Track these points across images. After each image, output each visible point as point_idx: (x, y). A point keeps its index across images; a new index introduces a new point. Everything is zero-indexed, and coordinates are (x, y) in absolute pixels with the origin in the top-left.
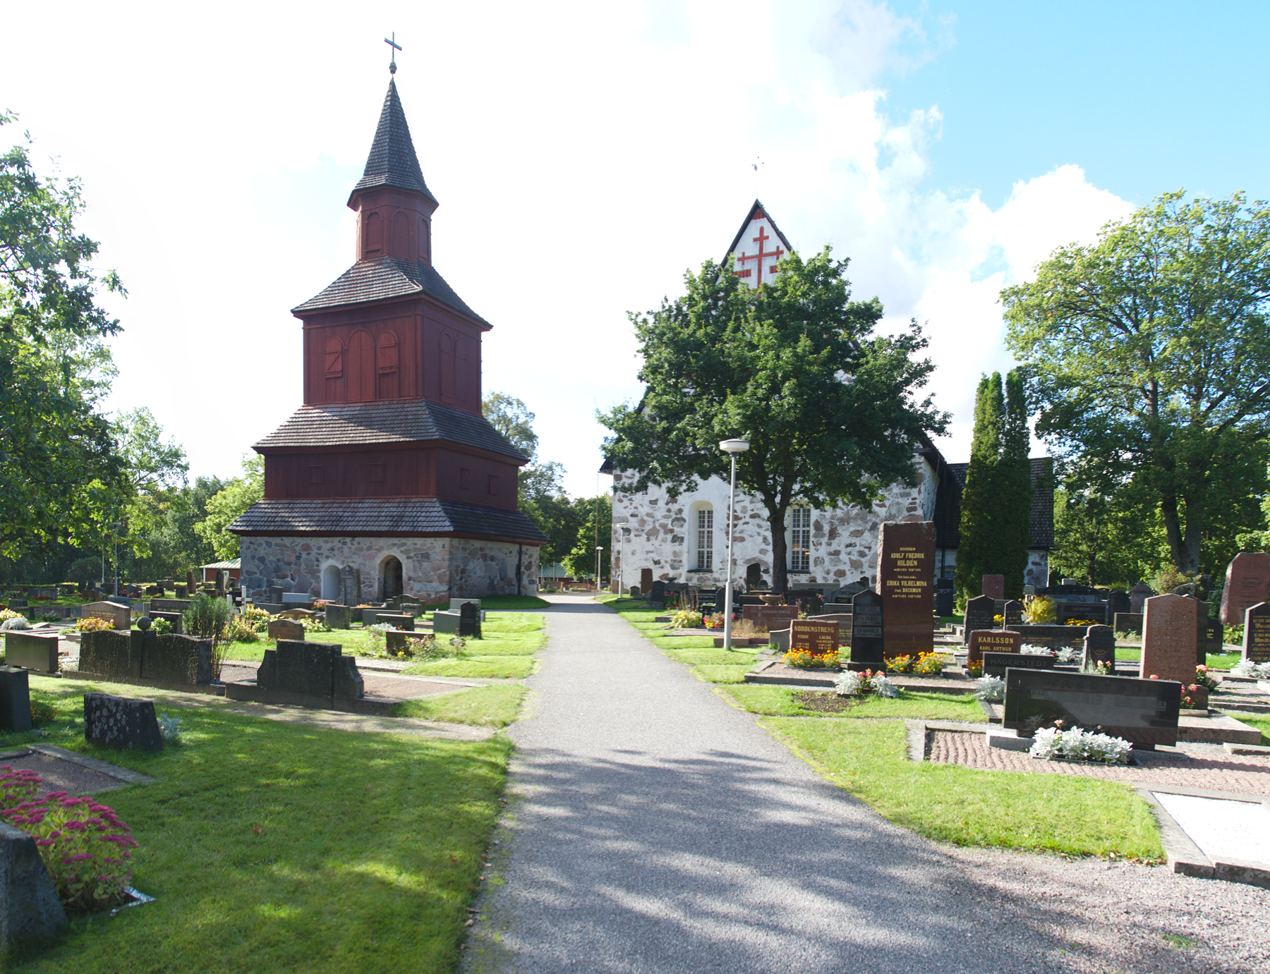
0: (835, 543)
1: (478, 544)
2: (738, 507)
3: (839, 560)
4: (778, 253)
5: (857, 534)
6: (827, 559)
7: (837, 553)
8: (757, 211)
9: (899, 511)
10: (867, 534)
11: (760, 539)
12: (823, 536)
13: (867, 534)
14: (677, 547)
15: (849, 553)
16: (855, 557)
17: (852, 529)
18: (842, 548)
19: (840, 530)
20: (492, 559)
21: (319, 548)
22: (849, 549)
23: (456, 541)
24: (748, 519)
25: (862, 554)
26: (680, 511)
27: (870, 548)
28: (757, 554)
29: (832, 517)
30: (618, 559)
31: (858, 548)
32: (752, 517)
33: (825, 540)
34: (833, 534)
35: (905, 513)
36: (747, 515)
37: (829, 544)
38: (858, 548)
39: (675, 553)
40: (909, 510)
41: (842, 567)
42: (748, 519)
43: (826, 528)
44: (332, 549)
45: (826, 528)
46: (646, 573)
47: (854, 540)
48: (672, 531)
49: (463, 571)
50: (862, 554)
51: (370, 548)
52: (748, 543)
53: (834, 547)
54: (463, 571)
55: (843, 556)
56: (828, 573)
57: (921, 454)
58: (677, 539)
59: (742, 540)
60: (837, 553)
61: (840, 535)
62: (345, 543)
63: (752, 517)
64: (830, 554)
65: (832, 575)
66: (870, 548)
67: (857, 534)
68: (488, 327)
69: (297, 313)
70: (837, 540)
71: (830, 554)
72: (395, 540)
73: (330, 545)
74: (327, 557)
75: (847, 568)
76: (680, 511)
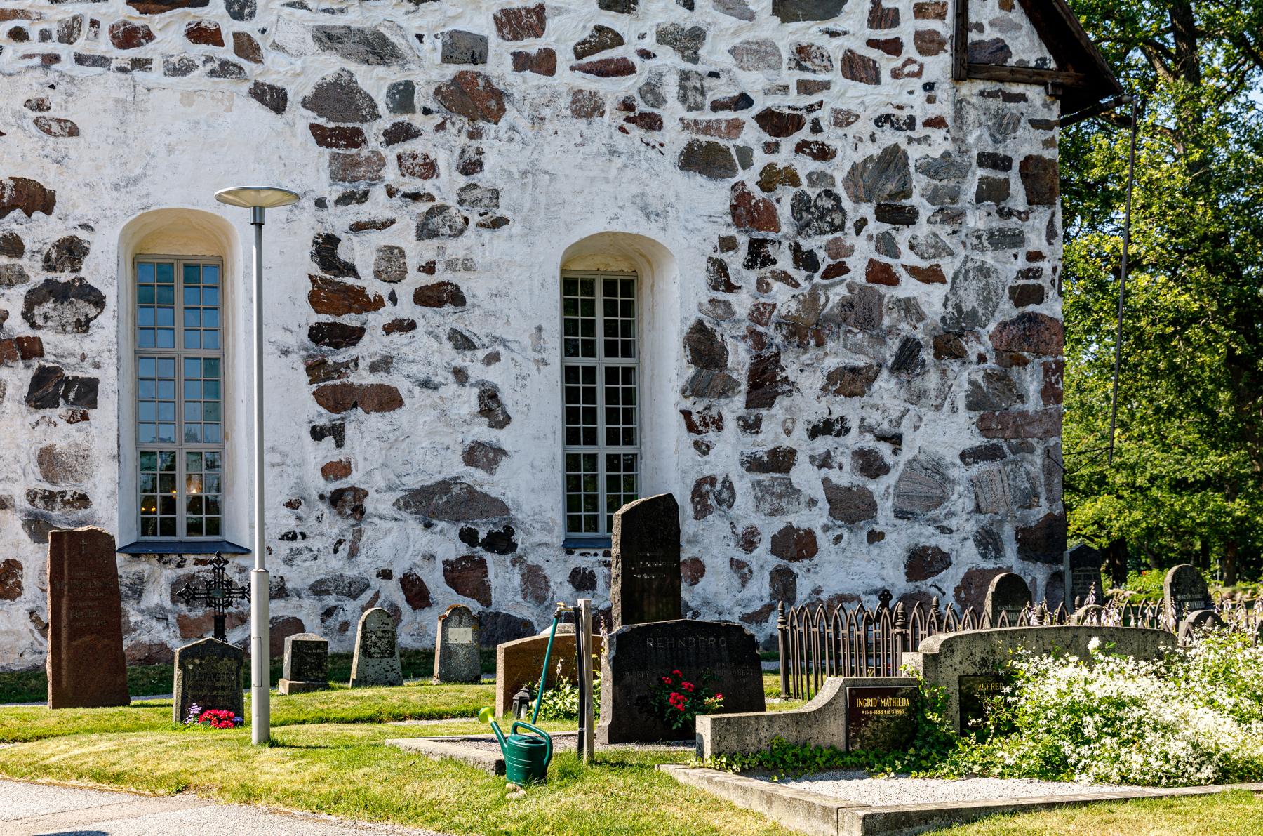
0: (774, 417)
2: (360, 253)
3: (791, 492)
5: (851, 382)
6: (743, 484)
7: (781, 461)
9: (987, 298)
10: (885, 385)
11: (469, 400)
12: (728, 389)
13: (885, 385)
14: (59, 431)
15: (825, 461)
16: (845, 476)
17: (832, 363)
18: (798, 440)
19: (791, 365)
22: (823, 444)
24: (406, 308)
25: (871, 465)
26: (72, 251)
28: (455, 467)
29: (759, 314)
31: (854, 440)
32: (425, 297)
33: (733, 407)
34: (765, 384)
35: (1008, 310)
36: (406, 290)
37: (751, 426)
38: (854, 440)
39: (48, 460)
41: (801, 519)
42: (406, 308)
43: (739, 358)
45: (739, 358)
47: (841, 407)
50: (871, 465)
52: (416, 414)
53: (770, 437)
55: (805, 476)
56: (749, 541)
58: (56, 390)
59: (388, 400)
60: (781, 461)
61: (793, 388)
63: (425, 297)
64: (753, 464)
65: (763, 548)
66: (896, 440)
67: (851, 382)
70: (781, 405)
71: (753, 464)
75: (815, 519)
76: (72, 251)
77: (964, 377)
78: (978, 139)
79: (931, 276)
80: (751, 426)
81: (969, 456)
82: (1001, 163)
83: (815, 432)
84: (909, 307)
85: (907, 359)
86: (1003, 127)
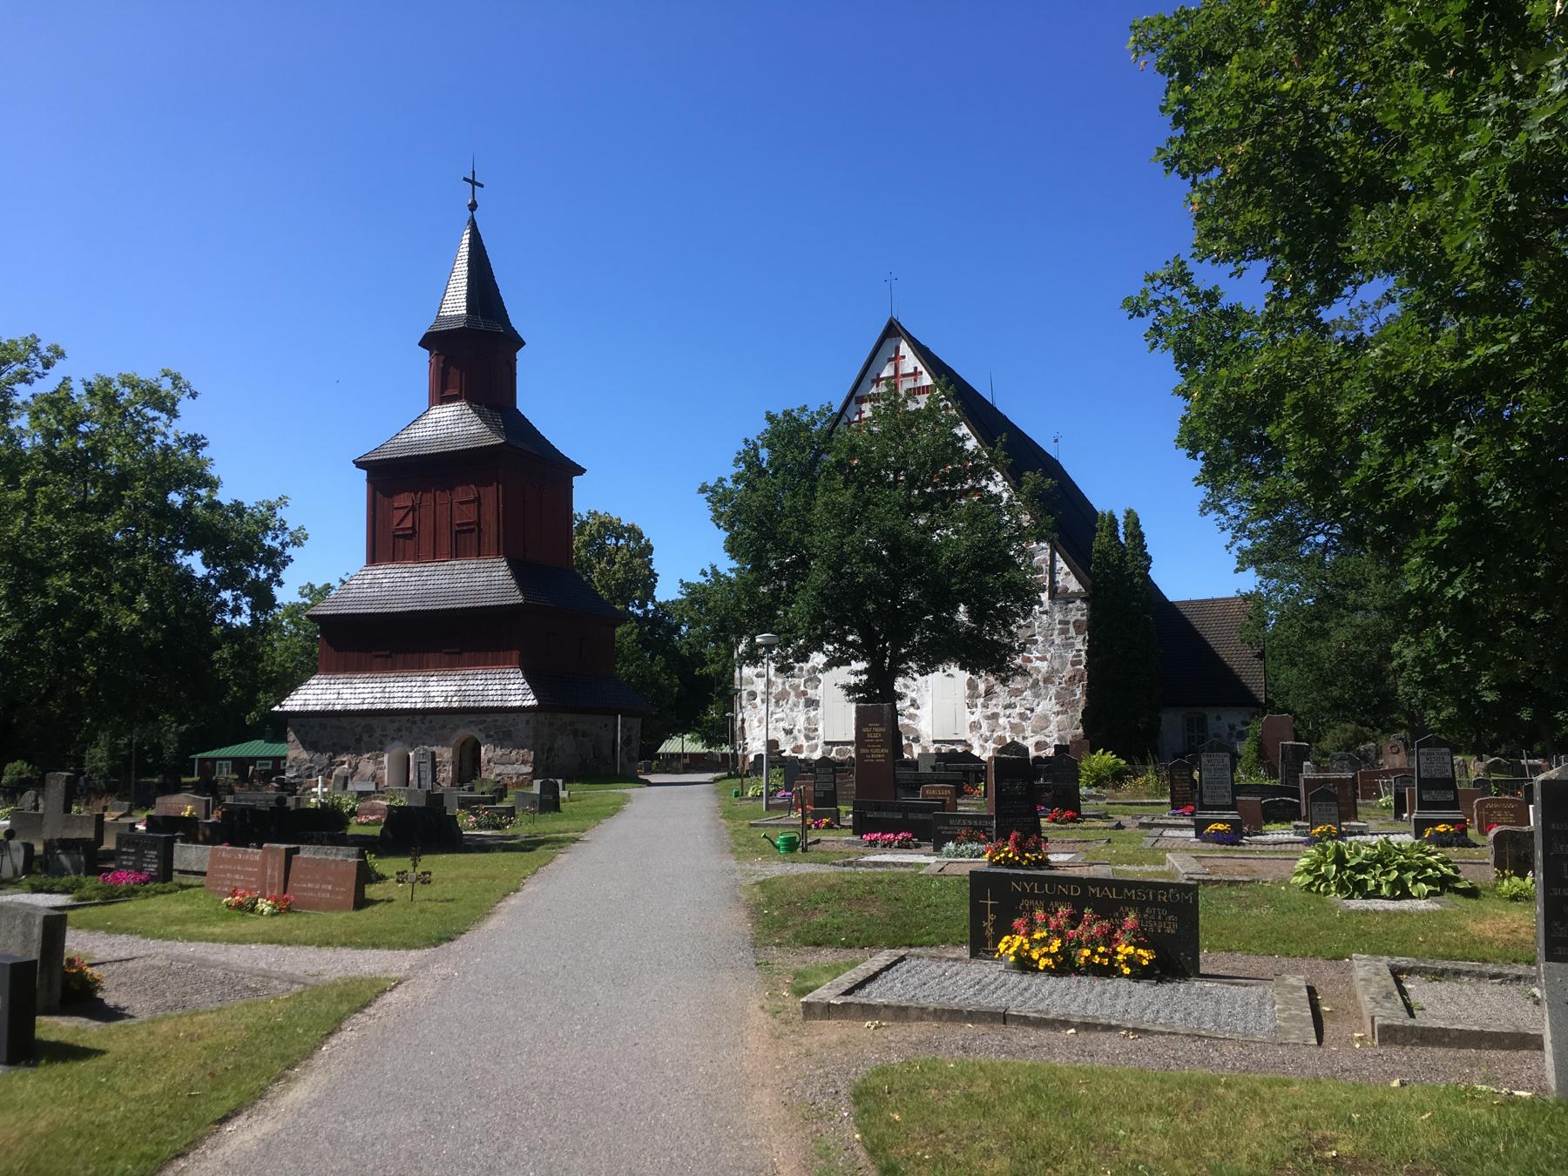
1: (567, 718)
4: (916, 374)
6: (985, 724)
7: (995, 716)
8: (893, 331)
10: (1027, 693)
16: (1016, 720)
18: (999, 710)
20: (584, 734)
21: (384, 729)
22: (1008, 711)
23: (541, 716)
27: (1032, 710)
30: (742, 728)
31: (1018, 710)
37: (985, 706)
38: (1018, 710)
40: (1074, 664)
44: (400, 730)
46: (772, 745)
48: (805, 693)
49: (550, 750)
50: (1022, 716)
51: (444, 727)
54: (550, 750)
55: (1002, 721)
57: (1084, 600)
60: (995, 716)
62: (414, 723)
64: (988, 718)
66: (1032, 710)
68: (580, 471)
69: (360, 464)
71: (988, 718)
72: (472, 718)
73: (396, 725)
74: (393, 739)
77: (1053, 690)
78: (1058, 616)
79: (1043, 659)
80: (985, 706)
81: (1058, 713)
82: (1067, 623)
83: (1006, 707)
84: (1038, 670)
85: (1036, 683)
86: (1067, 611)
